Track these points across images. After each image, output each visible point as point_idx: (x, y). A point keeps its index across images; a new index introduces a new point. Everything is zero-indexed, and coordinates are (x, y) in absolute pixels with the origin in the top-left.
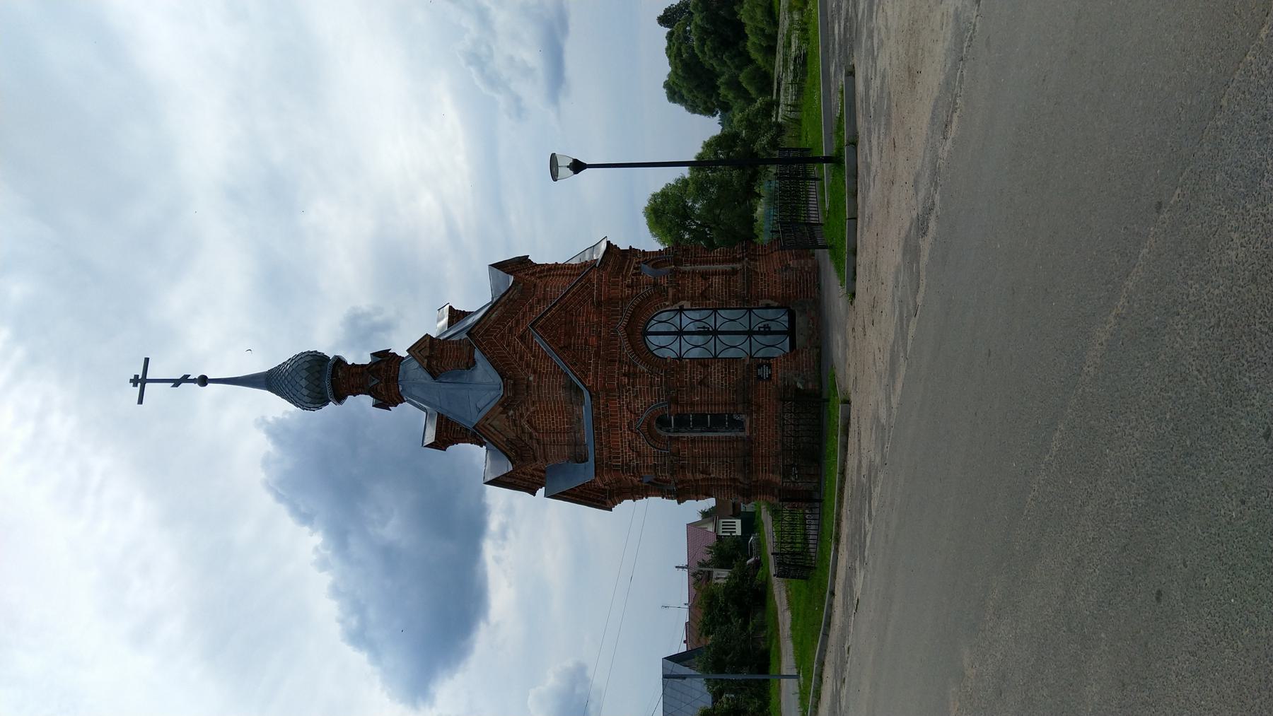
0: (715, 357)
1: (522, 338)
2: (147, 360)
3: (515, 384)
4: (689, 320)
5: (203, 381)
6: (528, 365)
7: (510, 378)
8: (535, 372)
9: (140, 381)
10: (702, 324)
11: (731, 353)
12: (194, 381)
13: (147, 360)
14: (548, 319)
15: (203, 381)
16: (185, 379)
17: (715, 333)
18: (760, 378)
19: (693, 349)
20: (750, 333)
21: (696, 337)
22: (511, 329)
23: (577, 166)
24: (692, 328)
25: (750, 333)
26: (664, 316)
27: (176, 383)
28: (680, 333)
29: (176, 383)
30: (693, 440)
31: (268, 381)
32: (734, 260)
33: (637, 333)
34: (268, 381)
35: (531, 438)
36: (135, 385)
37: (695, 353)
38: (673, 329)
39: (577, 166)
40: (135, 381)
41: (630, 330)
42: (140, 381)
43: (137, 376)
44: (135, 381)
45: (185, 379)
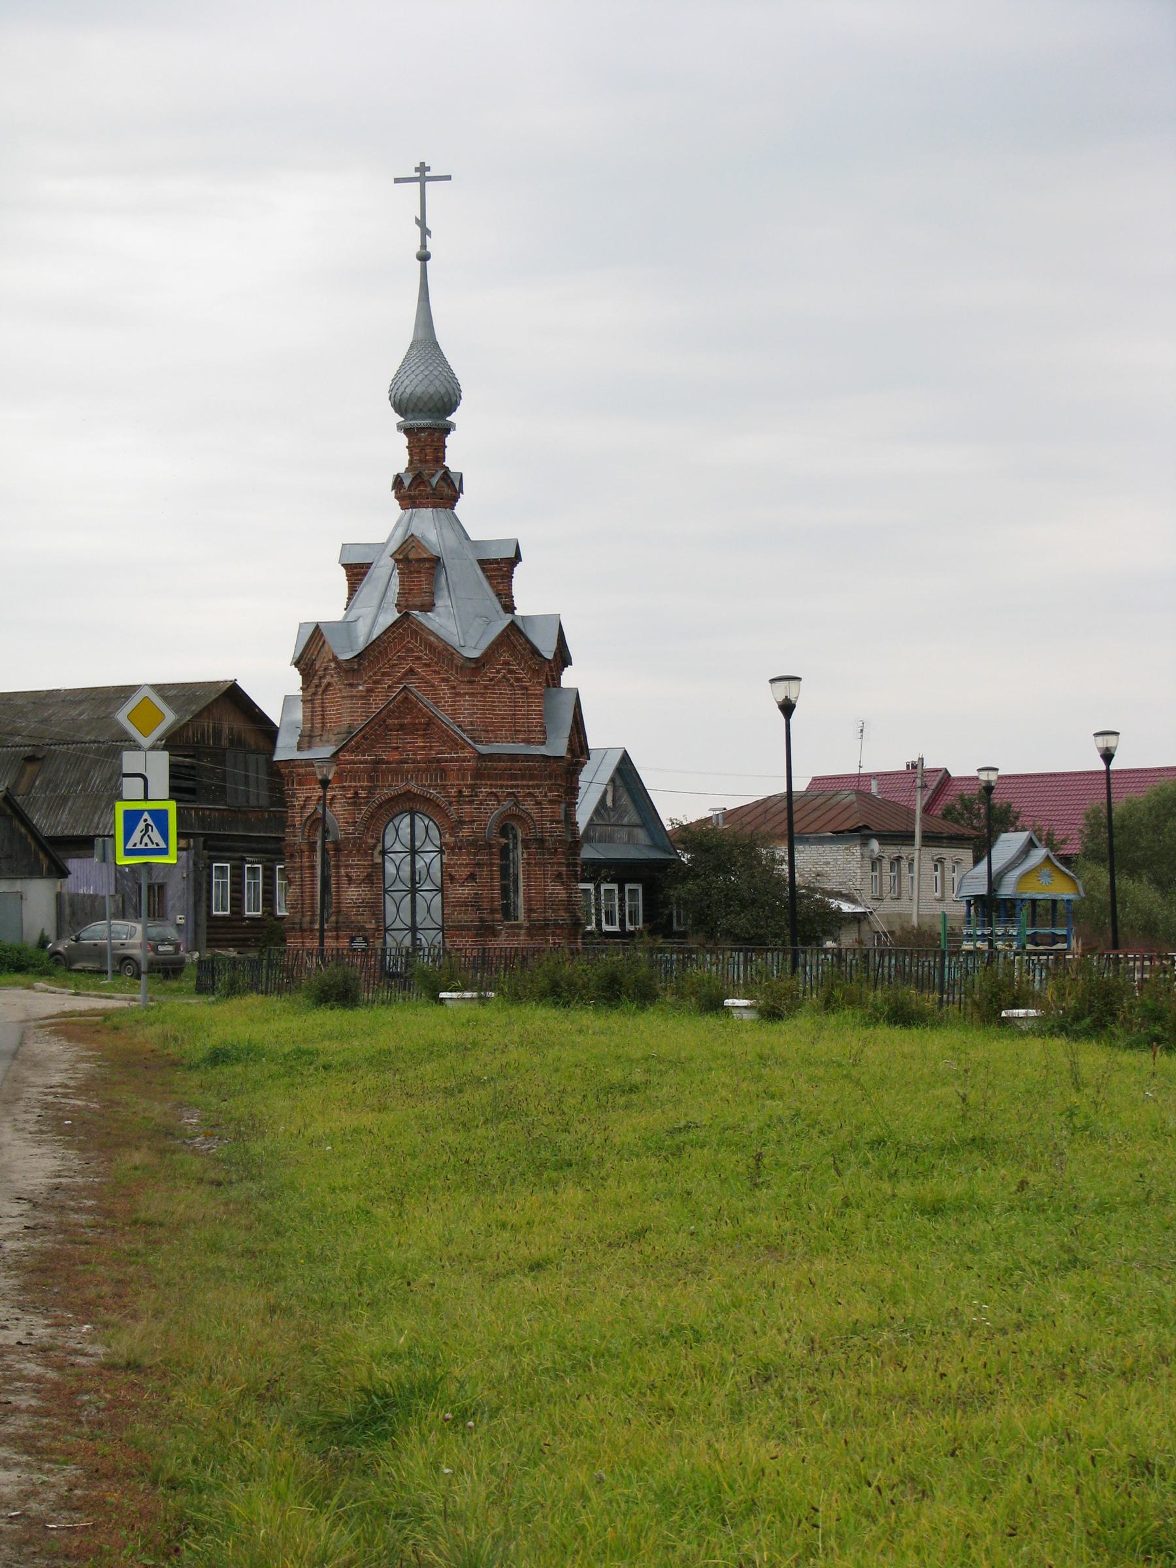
0: (386, 891)
1: (411, 670)
2: (448, 178)
3: (354, 670)
4: (430, 860)
5: (424, 257)
6: (376, 682)
7: (359, 665)
8: (369, 691)
9: (423, 175)
10: (424, 876)
11: (390, 908)
12: (424, 246)
13: (448, 178)
14: (86, 751)
15: (424, 257)
16: (425, 232)
17: (414, 891)
18: (353, 939)
19: (395, 866)
20: (414, 929)
21: (408, 869)
22: (419, 658)
23: (787, 708)
24: (420, 864)
25: (414, 929)
26: (434, 833)
27: (421, 222)
28: (413, 852)
29: (421, 222)
30: (313, 867)
31: (426, 342)
32: (529, 911)
33: (410, 803)
34: (426, 342)
35: (317, 686)
36: (417, 170)
37: (390, 869)
38: (418, 844)
39: (787, 708)
40: (423, 168)
41: (408, 796)
42: (423, 175)
43: (428, 169)
44: (423, 168)
45: (425, 232)
